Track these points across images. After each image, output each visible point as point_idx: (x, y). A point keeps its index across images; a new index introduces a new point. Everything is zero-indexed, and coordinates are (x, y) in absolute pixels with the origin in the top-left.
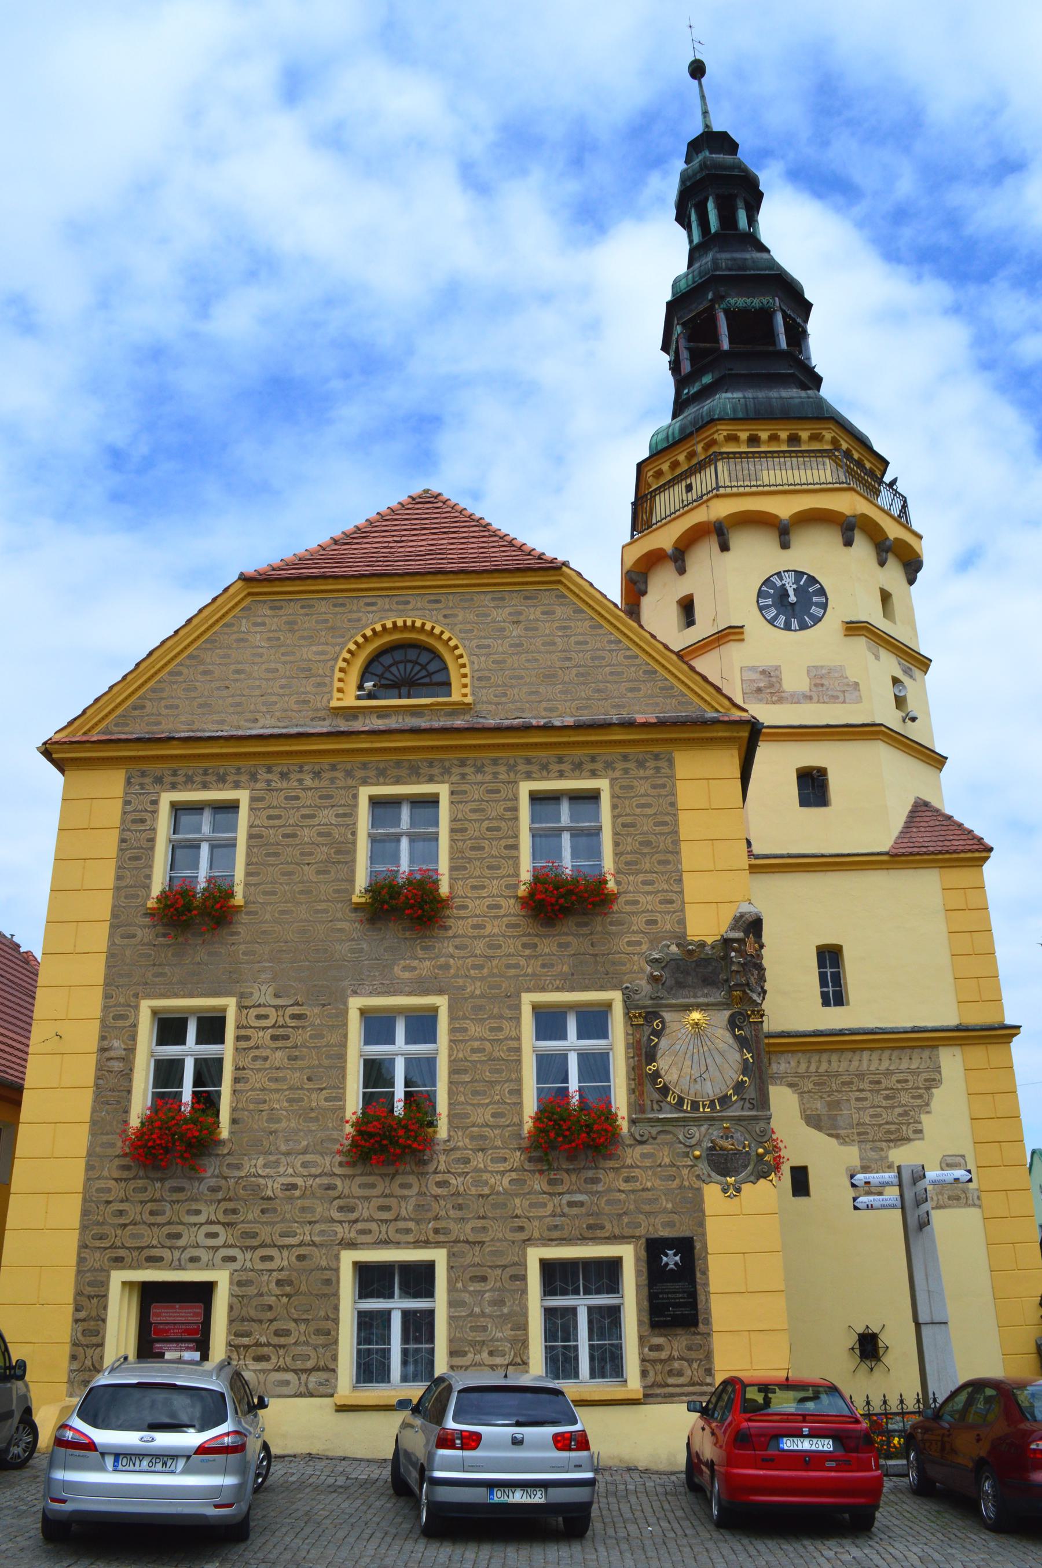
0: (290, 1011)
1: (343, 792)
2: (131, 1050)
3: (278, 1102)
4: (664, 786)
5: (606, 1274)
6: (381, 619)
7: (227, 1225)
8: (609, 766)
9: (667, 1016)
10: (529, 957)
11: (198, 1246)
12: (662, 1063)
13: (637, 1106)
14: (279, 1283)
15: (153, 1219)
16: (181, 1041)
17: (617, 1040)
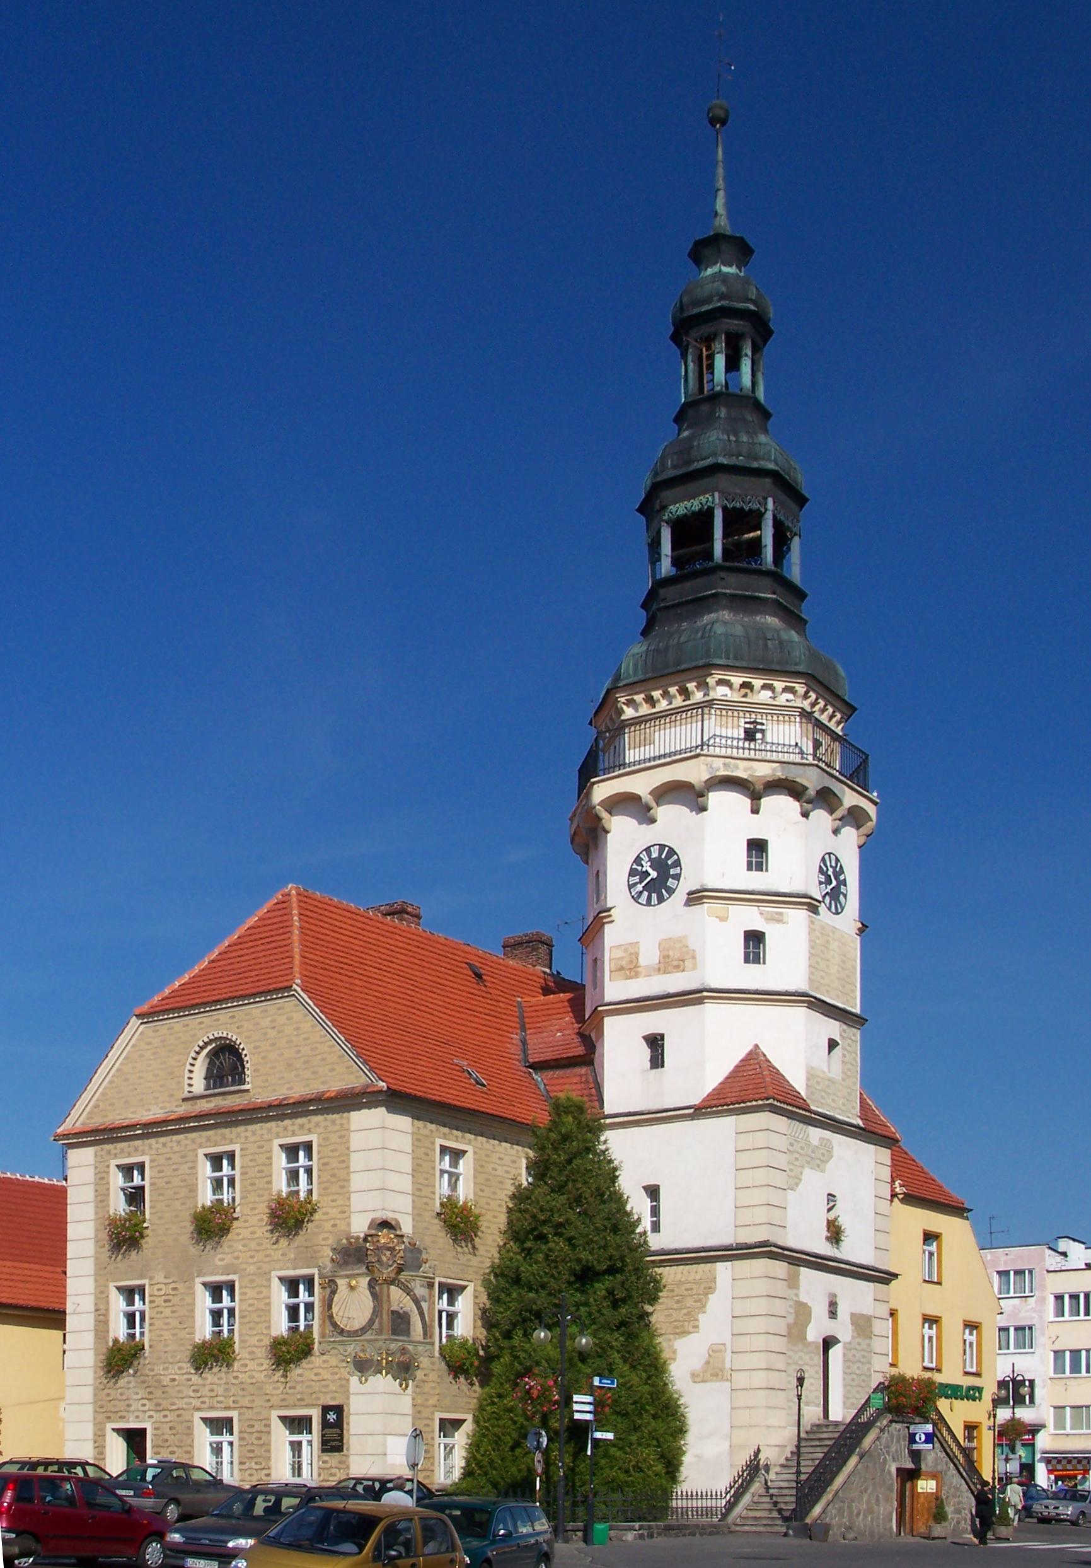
0: (171, 1286)
3: (167, 1335)
8: (317, 1125)
12: (335, 1310)
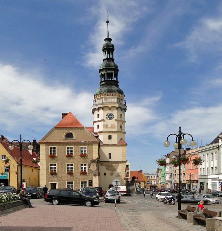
2: (49, 167)
5: (86, 182)
12: (90, 168)
13: (89, 171)
17: (87, 167)
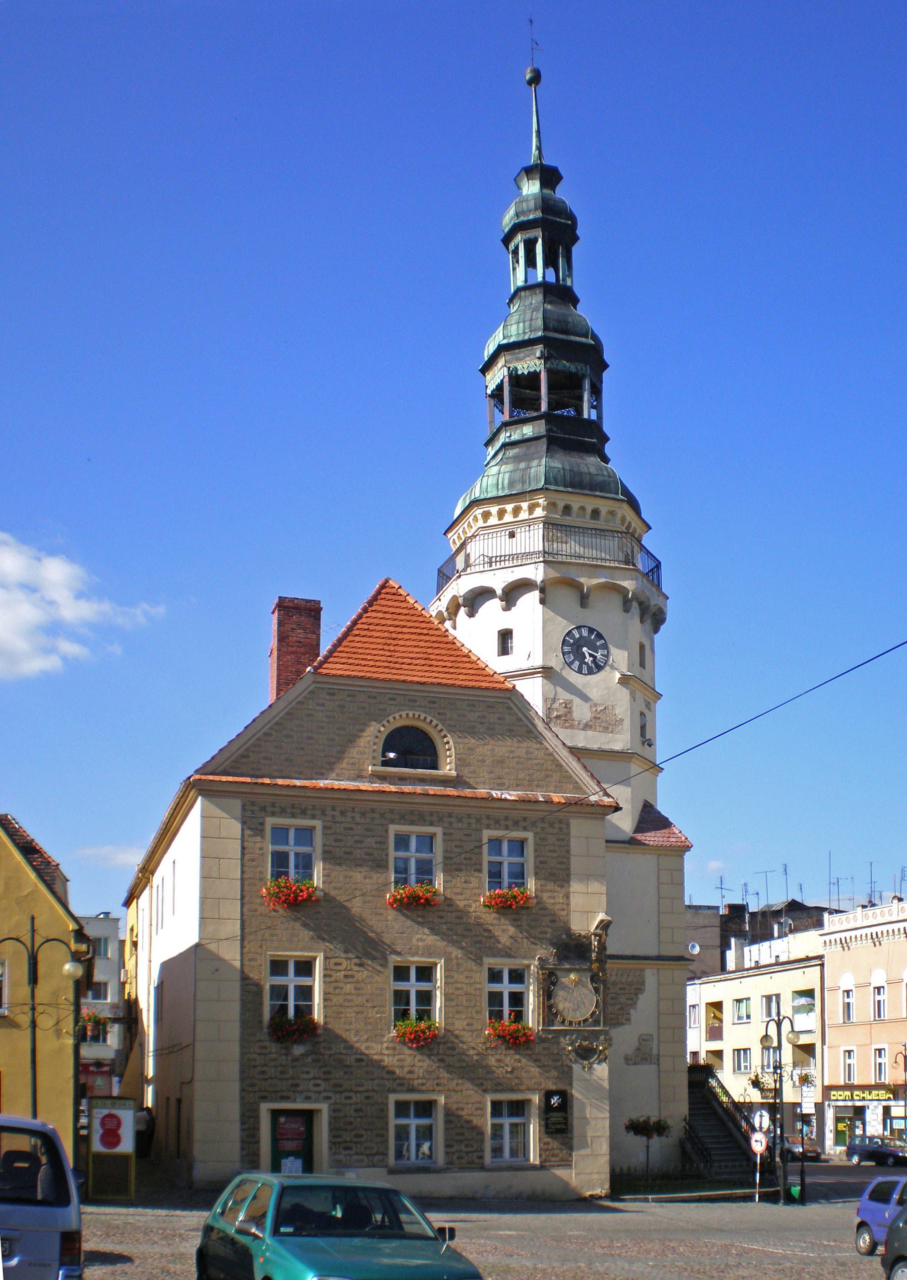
1: (380, 827)
4: (563, 840)
6: (399, 710)
7: (326, 1080)
9: (558, 973)
10: (487, 937)
11: (309, 1091)
14: (356, 1110)
15: (282, 1076)
16: (284, 973)
